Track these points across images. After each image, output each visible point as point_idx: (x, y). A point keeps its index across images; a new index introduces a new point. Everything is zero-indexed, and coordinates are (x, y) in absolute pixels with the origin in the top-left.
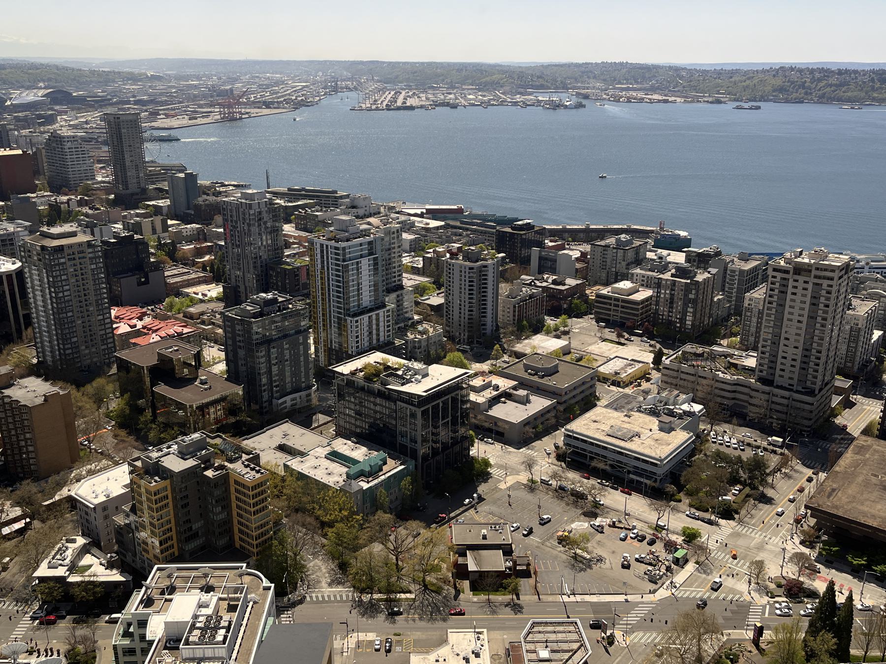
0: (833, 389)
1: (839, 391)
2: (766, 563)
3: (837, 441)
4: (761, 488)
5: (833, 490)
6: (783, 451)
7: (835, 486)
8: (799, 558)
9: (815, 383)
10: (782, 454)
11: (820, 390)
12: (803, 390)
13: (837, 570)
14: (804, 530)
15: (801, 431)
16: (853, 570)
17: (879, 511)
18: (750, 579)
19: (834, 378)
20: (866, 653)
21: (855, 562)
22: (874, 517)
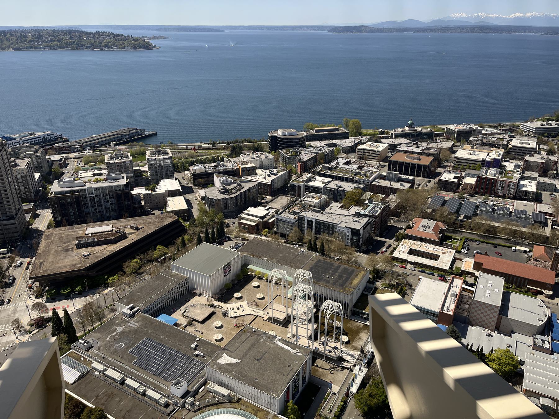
0: (24, 211)
1: (28, 211)
2: (20, 318)
3: (37, 237)
4: (4, 280)
5: (41, 263)
6: (9, 255)
7: (41, 261)
8: (37, 306)
9: (11, 212)
10: (9, 257)
11: (16, 214)
12: (7, 218)
13: (59, 301)
14: (34, 291)
15: (15, 240)
16: (66, 297)
17: (67, 263)
18: (14, 331)
19: (21, 205)
20: (85, 331)
21: (65, 293)
22: (65, 267)
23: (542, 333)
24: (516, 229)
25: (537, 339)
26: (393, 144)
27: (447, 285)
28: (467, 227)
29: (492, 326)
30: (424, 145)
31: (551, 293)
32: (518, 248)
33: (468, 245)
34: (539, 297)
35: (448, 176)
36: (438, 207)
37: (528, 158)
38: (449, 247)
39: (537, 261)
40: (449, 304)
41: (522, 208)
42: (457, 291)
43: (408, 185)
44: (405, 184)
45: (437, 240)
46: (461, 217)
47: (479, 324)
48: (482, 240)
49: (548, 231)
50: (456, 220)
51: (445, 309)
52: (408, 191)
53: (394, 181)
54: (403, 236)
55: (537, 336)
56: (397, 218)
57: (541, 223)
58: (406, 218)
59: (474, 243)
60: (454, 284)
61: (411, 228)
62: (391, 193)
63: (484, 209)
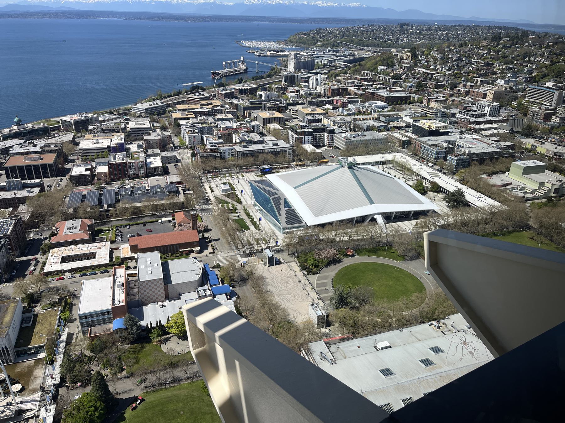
23: (202, 284)
24: (156, 203)
25: (200, 291)
26: (4, 147)
27: (112, 278)
28: (114, 216)
29: (162, 297)
30: (41, 143)
31: (199, 248)
32: (163, 219)
33: (121, 232)
34: (192, 255)
35: (79, 170)
36: (79, 204)
37: (147, 137)
38: (103, 240)
39: (181, 226)
40: (118, 296)
41: (155, 184)
42: (122, 280)
43: (38, 189)
44: (33, 190)
45: (88, 237)
46: (106, 207)
47: (151, 301)
48: (132, 223)
49: (181, 198)
50: (101, 211)
51: (116, 302)
52: (39, 196)
53: (18, 189)
54: (49, 247)
55: (200, 288)
56: (36, 229)
57: (174, 192)
58: (48, 225)
59: (125, 228)
60: (118, 275)
61: (56, 235)
62: (19, 204)
63: (124, 193)
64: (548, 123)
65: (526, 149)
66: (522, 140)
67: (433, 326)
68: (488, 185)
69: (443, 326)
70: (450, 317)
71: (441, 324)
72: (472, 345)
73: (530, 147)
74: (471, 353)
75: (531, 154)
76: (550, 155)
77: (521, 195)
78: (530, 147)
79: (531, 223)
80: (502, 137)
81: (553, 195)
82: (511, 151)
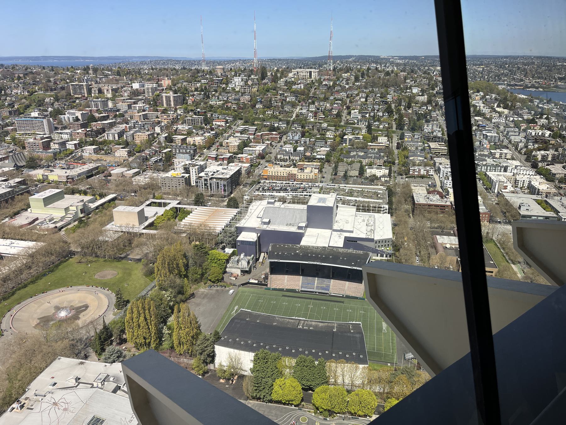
64: (49, 151)
65: (39, 181)
66: (30, 173)
67: (15, 409)
68: (15, 228)
69: (26, 402)
70: (29, 387)
71: (23, 401)
72: (62, 400)
73: (41, 178)
74: (65, 410)
75: (45, 184)
76: (63, 180)
77: (53, 226)
78: (41, 178)
79: (73, 248)
80: (8, 176)
81: (82, 216)
82: (23, 187)
